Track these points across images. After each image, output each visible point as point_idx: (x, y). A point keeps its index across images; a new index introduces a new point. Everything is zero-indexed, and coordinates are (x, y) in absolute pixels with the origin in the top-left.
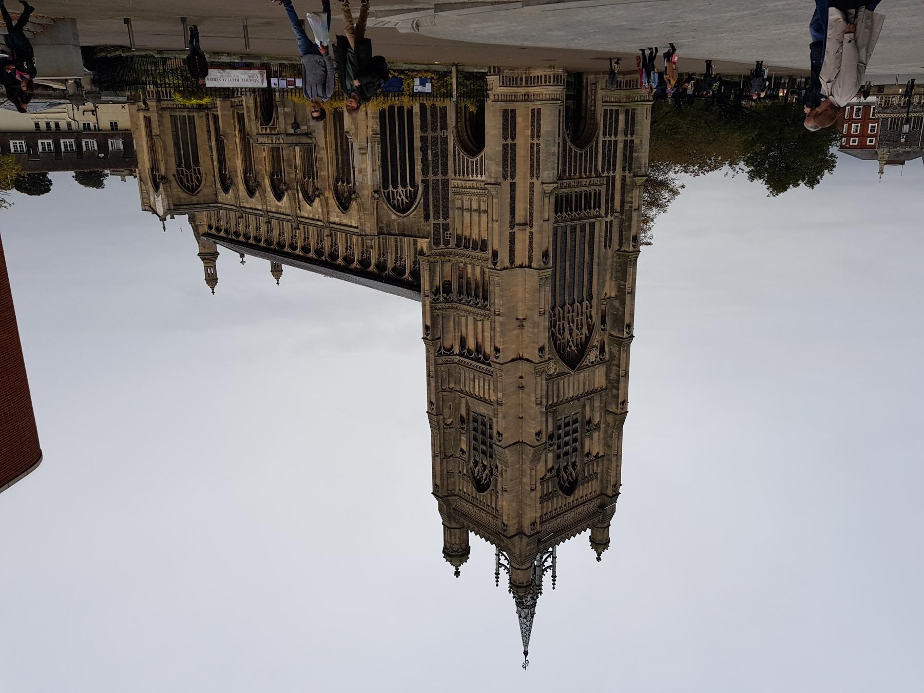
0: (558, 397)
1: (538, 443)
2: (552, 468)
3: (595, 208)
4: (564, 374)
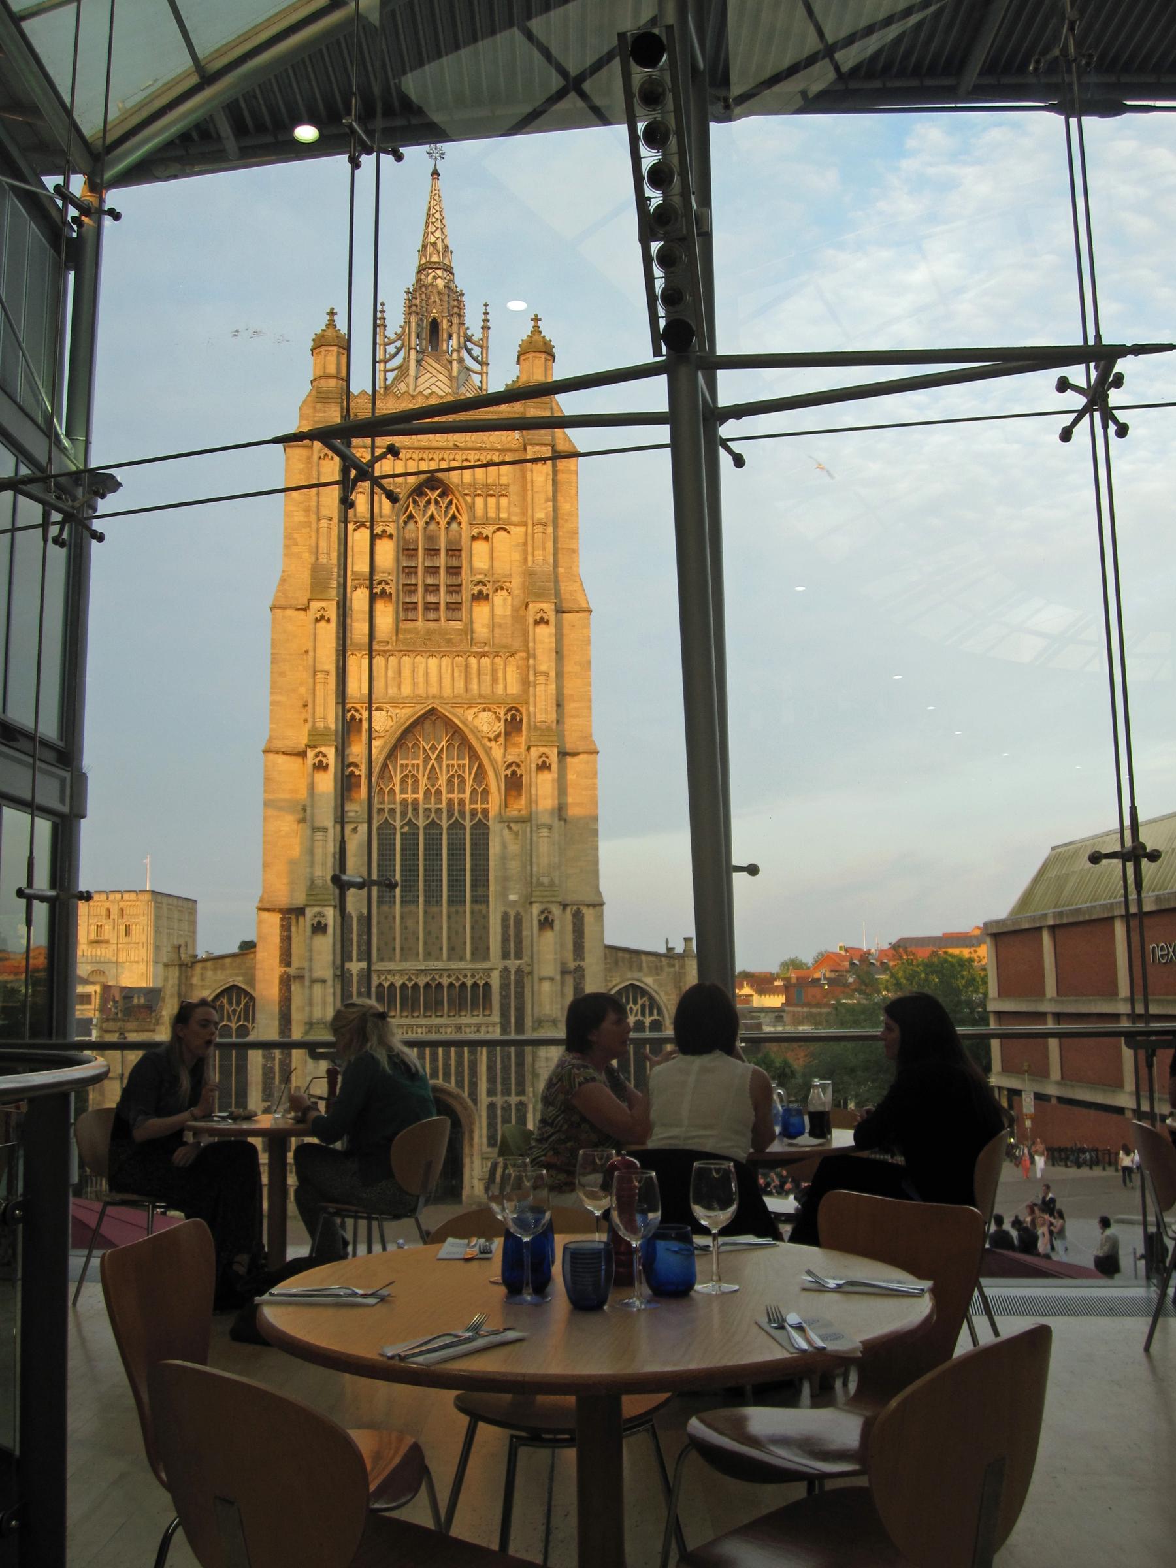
0: (467, 667)
1: (544, 606)
2: (474, 538)
3: (392, 985)
4: (455, 705)
